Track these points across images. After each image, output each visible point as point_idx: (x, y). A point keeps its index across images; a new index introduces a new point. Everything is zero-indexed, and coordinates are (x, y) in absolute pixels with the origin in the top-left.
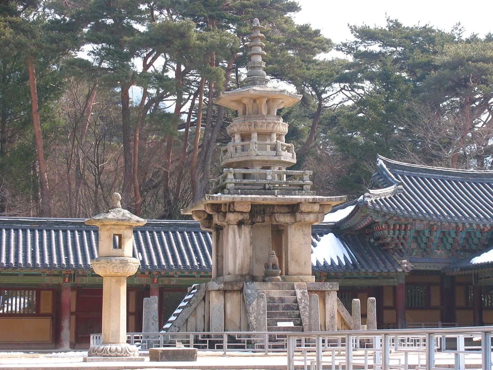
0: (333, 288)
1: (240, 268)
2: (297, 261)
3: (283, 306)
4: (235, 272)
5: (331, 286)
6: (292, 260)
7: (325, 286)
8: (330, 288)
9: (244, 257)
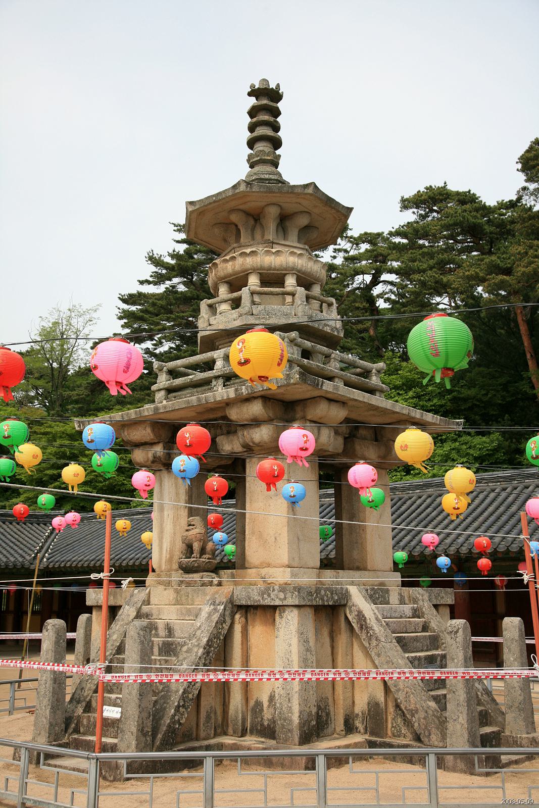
0: (285, 598)
1: (168, 556)
2: (261, 536)
3: (160, 645)
4: (160, 567)
5: (282, 595)
6: (253, 533)
7: (269, 595)
8: (280, 599)
9: (175, 534)
